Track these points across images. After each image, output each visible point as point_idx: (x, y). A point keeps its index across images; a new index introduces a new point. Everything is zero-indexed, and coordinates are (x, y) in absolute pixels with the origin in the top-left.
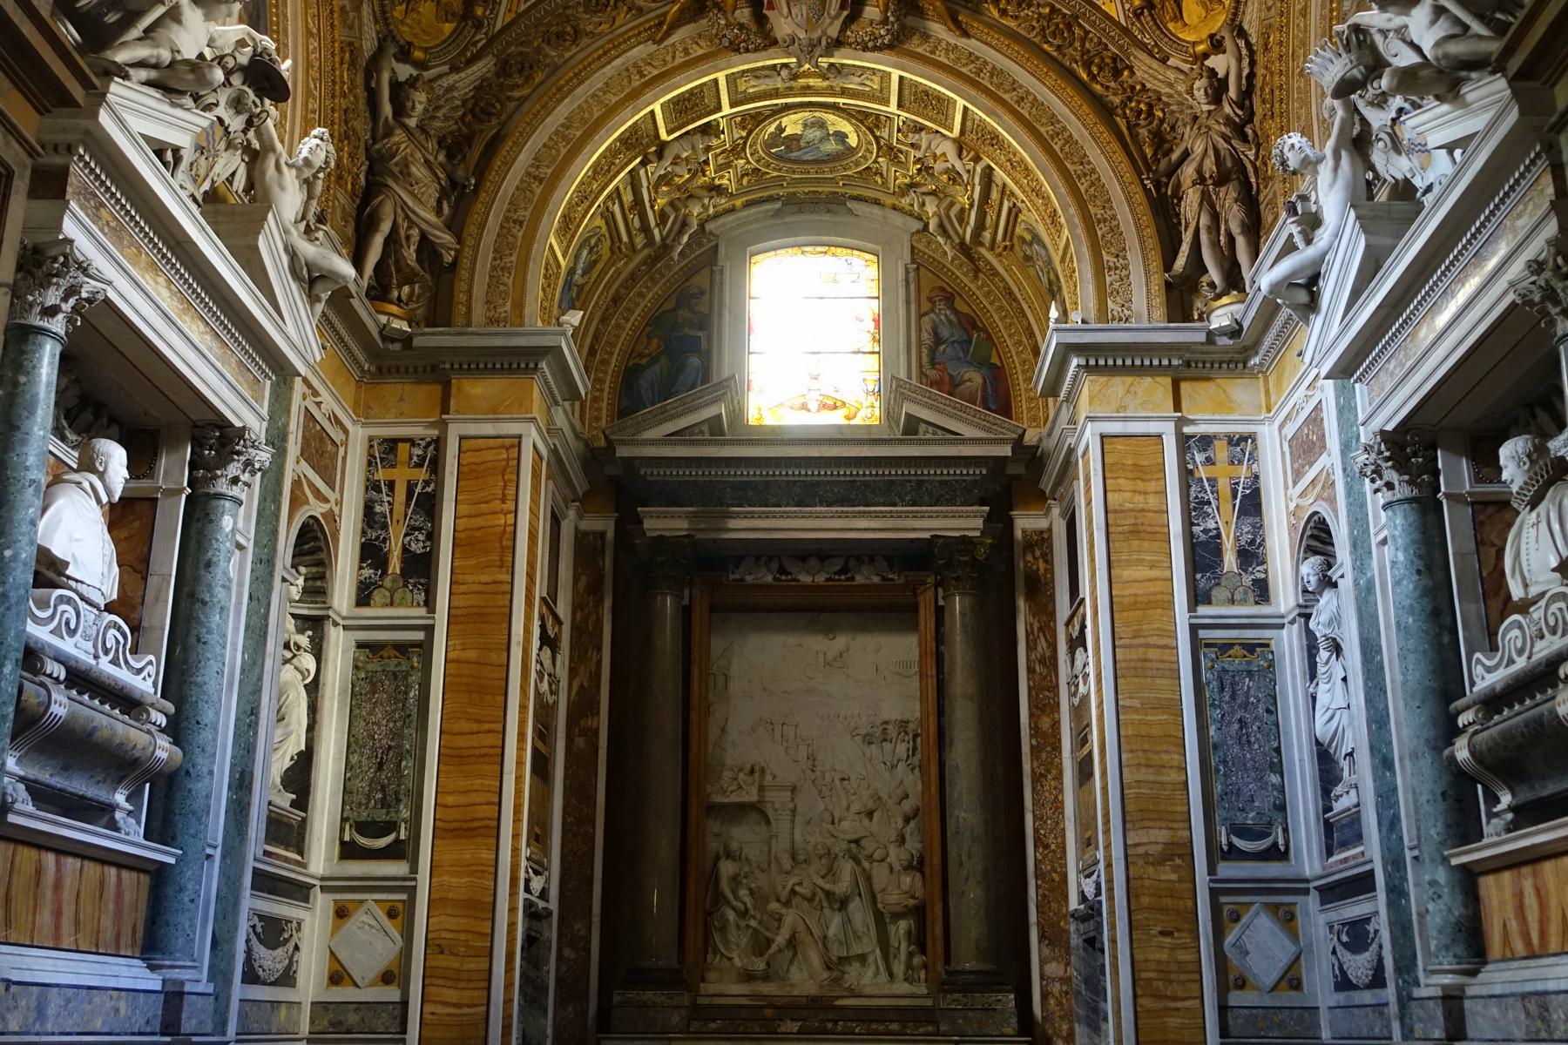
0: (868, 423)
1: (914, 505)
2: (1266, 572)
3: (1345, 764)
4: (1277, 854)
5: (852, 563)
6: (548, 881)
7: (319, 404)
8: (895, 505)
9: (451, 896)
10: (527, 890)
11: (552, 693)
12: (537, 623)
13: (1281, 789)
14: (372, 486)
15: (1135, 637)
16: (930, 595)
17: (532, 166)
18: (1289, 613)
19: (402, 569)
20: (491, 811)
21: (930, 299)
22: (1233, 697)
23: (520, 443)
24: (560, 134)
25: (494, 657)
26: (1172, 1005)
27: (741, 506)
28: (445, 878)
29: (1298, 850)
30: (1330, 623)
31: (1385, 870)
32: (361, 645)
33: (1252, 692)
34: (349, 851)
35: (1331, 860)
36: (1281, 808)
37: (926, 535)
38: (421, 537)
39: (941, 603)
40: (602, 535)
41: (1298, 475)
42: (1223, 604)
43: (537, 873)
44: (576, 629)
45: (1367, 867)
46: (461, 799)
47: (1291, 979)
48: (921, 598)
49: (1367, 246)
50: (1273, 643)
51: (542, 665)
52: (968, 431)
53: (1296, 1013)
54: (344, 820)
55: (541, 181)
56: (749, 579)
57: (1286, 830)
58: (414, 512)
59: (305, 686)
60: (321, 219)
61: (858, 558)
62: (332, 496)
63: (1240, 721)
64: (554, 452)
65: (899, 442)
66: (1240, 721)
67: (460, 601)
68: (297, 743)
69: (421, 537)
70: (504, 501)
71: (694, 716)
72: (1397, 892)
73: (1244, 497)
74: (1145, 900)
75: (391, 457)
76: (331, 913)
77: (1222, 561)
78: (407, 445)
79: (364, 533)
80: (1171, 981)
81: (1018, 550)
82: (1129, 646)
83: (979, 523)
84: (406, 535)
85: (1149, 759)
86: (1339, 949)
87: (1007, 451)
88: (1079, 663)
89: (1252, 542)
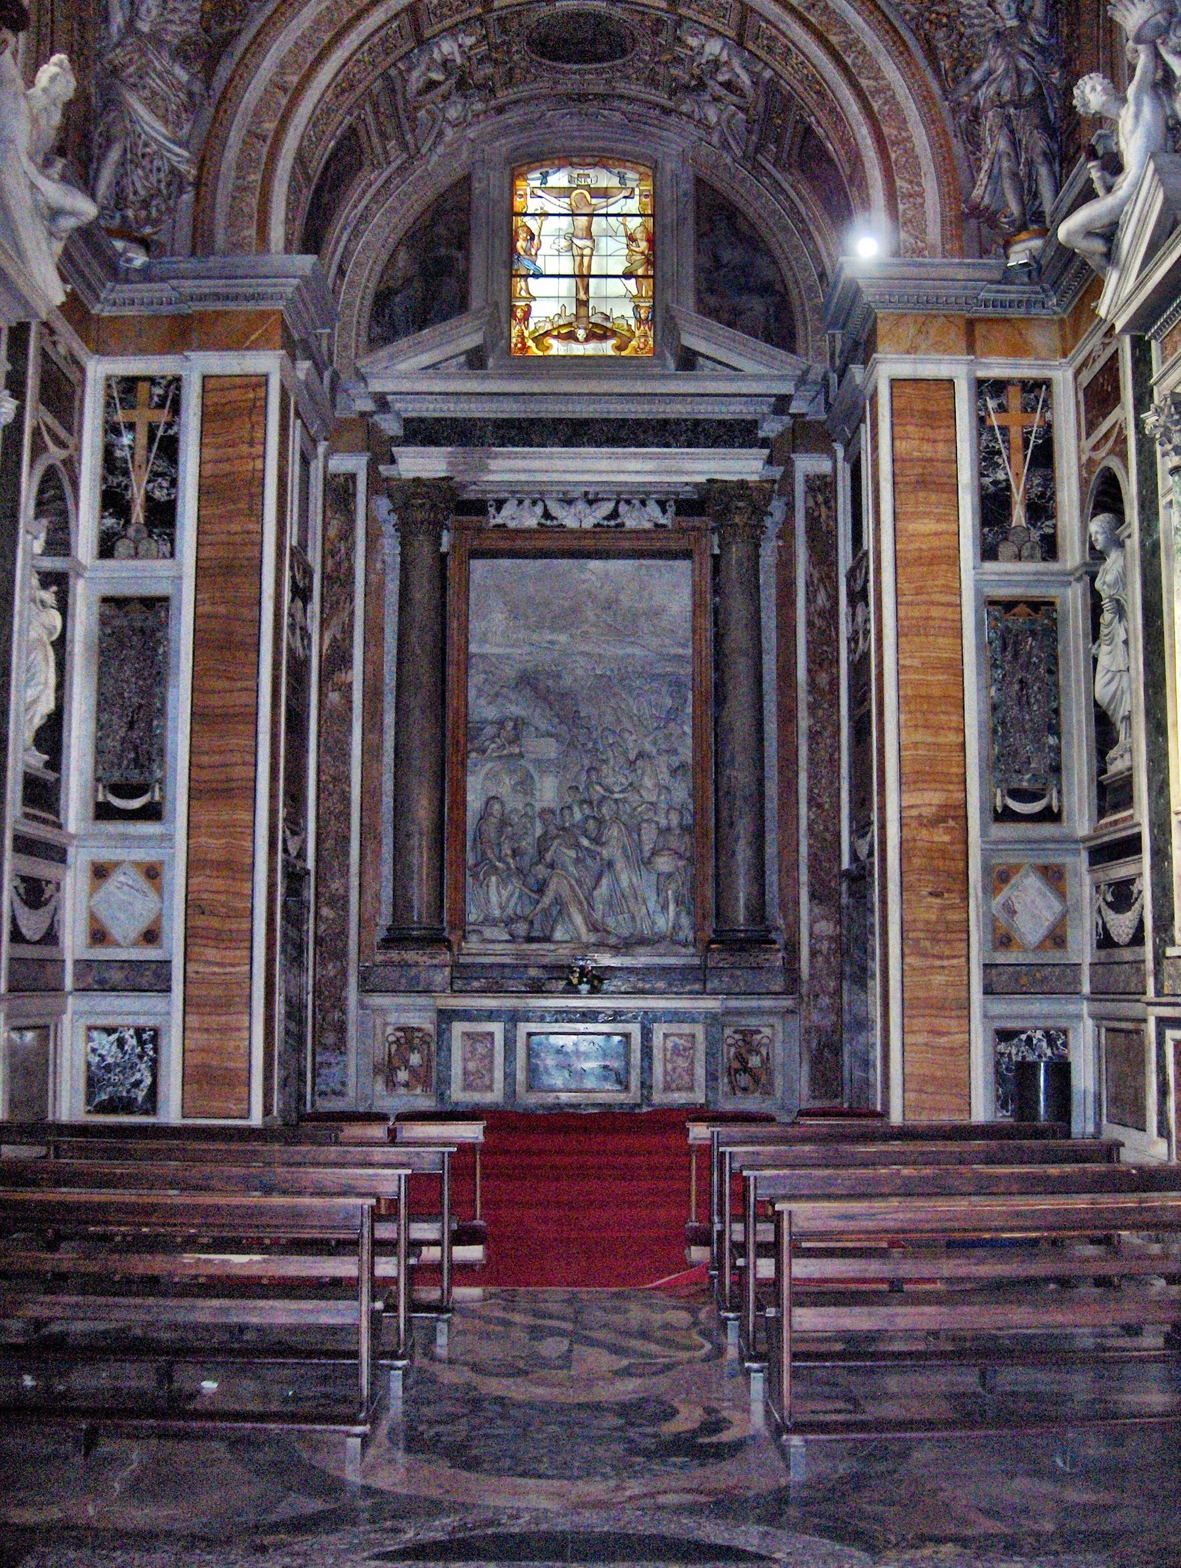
1: (689, 446)
2: (1055, 527)
3: (1122, 728)
4: (1050, 816)
7: (54, 343)
8: (668, 445)
9: (209, 857)
10: (285, 851)
12: (287, 574)
13: (1057, 750)
14: (112, 429)
17: (277, 74)
18: (1076, 569)
19: (147, 519)
20: (246, 771)
21: (710, 220)
22: (1016, 655)
23: (266, 383)
24: (305, 41)
25: (246, 613)
26: (938, 963)
27: (503, 445)
28: (203, 840)
29: (1070, 813)
30: (1116, 582)
31: (1151, 831)
32: (105, 600)
33: (1035, 652)
34: (103, 812)
35: (1103, 822)
36: (1056, 769)
37: (702, 479)
38: (165, 484)
41: (1091, 426)
42: (1008, 560)
43: (294, 833)
45: (1136, 830)
46: (216, 759)
47: (1057, 938)
49: (1166, 200)
50: (1058, 601)
52: (749, 366)
53: (1057, 970)
54: (98, 780)
55: (285, 90)
57: (1059, 792)
58: (157, 457)
59: (52, 643)
60: (61, 151)
62: (71, 442)
63: (1021, 681)
66: (1021, 681)
67: (207, 552)
68: (47, 704)
69: (165, 484)
70: (251, 444)
71: (451, 671)
72: (1161, 854)
73: (1035, 447)
74: (917, 862)
75: (130, 397)
76: (89, 874)
77: (1010, 515)
78: (146, 385)
79: (104, 479)
82: (911, 604)
84: (149, 482)
86: (1104, 907)
88: (860, 619)
89: (1042, 495)
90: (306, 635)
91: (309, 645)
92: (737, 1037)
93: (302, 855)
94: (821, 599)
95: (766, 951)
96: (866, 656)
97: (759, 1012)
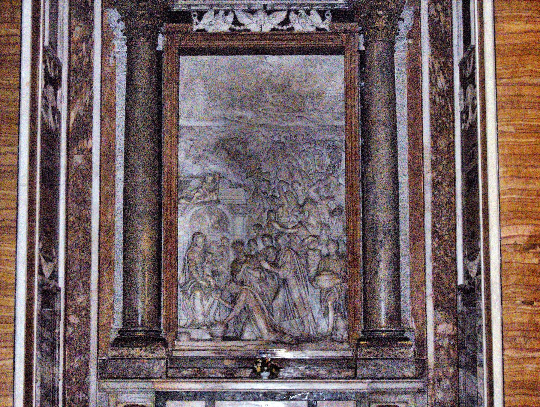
10: (41, 273)
12: (41, 67)
15: (512, 77)
26: (530, 355)
43: (48, 260)
51: (46, 99)
71: (166, 139)
80: (530, 338)
82: (507, 85)
85: (519, 172)
88: (469, 98)
90: (56, 112)
91: (59, 120)
93: (54, 276)
94: (441, 82)
95: (402, 346)
97: (399, 392)
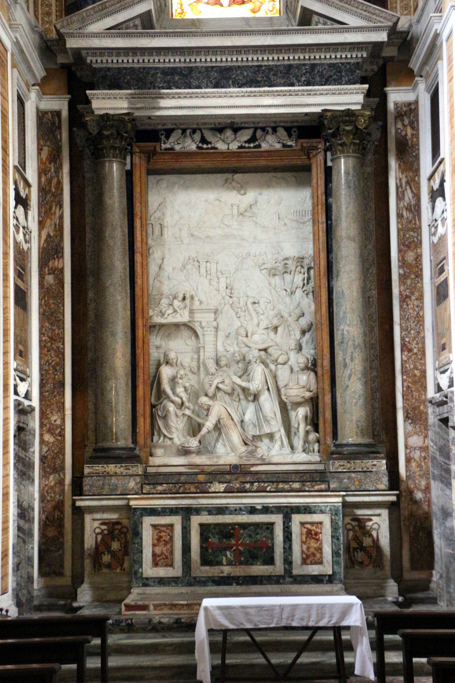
0: (270, 15)
1: (308, 84)
5: (259, 133)
6: (30, 385)
8: (292, 85)
10: (16, 393)
11: (26, 241)
16: (320, 157)
27: (170, 88)
37: (318, 110)
39: (329, 164)
40: (58, 114)
43: (22, 380)
44: (43, 191)
48: (313, 161)
56: (178, 148)
61: (263, 129)
64: (17, 44)
65: (297, 32)
71: (138, 258)
81: (390, 119)
83: (360, 98)
87: (382, 37)
88: (438, 209)
92: (354, 523)
93: (27, 396)
96: (443, 238)
